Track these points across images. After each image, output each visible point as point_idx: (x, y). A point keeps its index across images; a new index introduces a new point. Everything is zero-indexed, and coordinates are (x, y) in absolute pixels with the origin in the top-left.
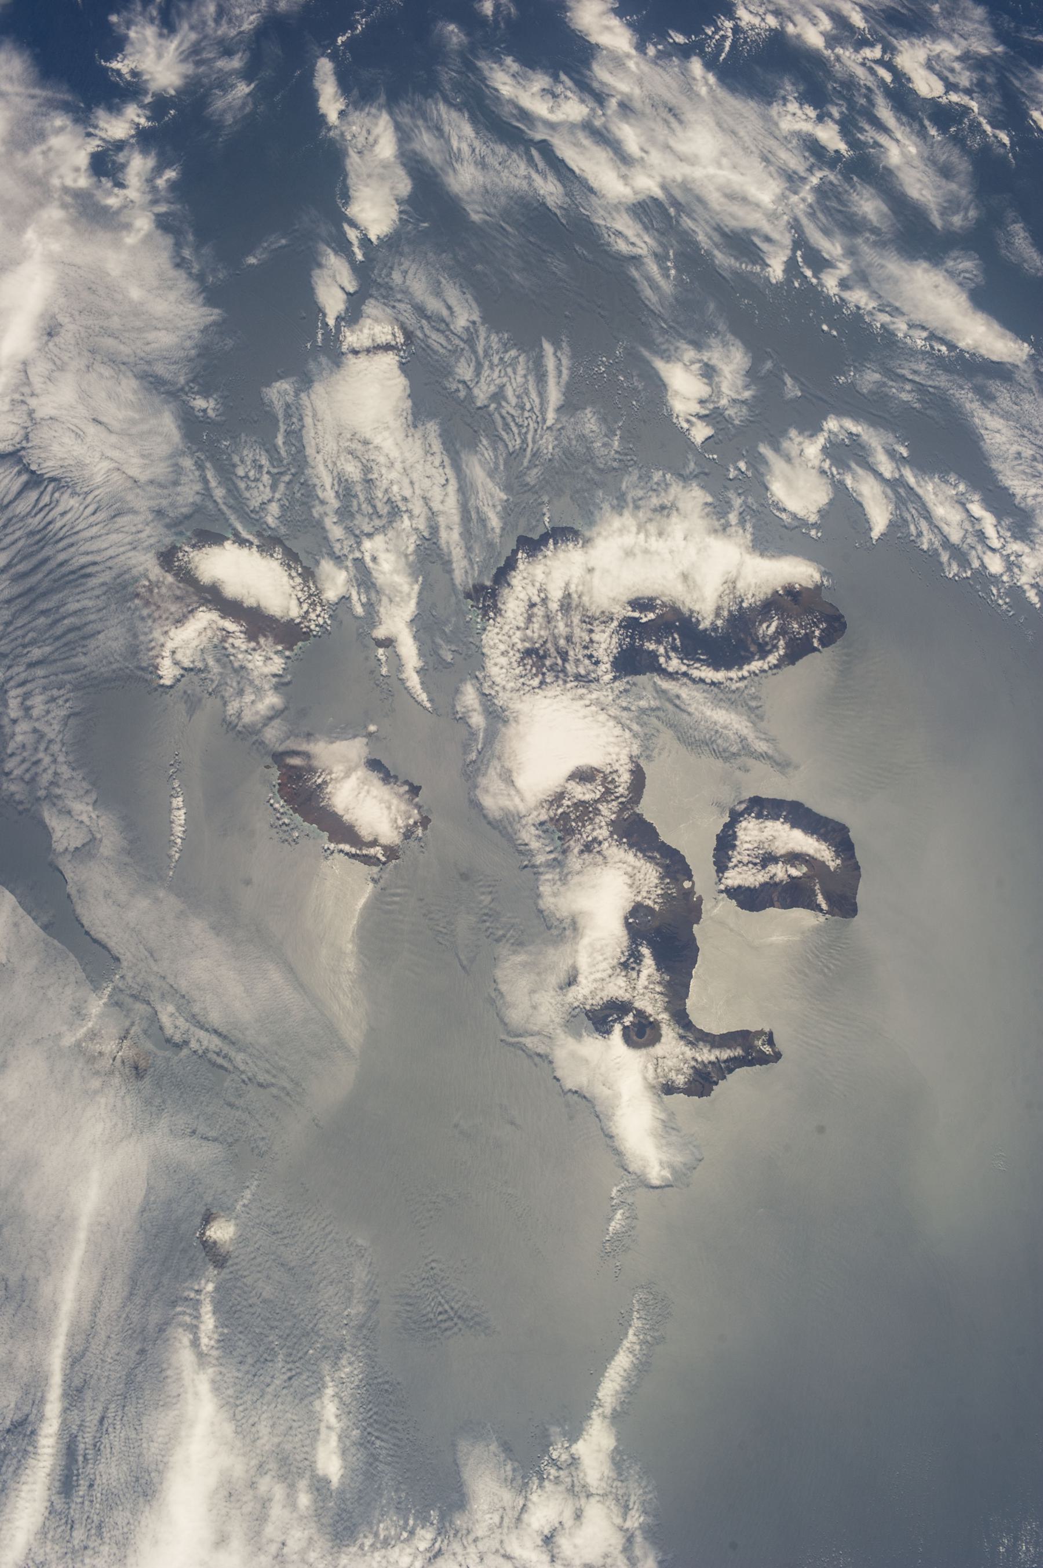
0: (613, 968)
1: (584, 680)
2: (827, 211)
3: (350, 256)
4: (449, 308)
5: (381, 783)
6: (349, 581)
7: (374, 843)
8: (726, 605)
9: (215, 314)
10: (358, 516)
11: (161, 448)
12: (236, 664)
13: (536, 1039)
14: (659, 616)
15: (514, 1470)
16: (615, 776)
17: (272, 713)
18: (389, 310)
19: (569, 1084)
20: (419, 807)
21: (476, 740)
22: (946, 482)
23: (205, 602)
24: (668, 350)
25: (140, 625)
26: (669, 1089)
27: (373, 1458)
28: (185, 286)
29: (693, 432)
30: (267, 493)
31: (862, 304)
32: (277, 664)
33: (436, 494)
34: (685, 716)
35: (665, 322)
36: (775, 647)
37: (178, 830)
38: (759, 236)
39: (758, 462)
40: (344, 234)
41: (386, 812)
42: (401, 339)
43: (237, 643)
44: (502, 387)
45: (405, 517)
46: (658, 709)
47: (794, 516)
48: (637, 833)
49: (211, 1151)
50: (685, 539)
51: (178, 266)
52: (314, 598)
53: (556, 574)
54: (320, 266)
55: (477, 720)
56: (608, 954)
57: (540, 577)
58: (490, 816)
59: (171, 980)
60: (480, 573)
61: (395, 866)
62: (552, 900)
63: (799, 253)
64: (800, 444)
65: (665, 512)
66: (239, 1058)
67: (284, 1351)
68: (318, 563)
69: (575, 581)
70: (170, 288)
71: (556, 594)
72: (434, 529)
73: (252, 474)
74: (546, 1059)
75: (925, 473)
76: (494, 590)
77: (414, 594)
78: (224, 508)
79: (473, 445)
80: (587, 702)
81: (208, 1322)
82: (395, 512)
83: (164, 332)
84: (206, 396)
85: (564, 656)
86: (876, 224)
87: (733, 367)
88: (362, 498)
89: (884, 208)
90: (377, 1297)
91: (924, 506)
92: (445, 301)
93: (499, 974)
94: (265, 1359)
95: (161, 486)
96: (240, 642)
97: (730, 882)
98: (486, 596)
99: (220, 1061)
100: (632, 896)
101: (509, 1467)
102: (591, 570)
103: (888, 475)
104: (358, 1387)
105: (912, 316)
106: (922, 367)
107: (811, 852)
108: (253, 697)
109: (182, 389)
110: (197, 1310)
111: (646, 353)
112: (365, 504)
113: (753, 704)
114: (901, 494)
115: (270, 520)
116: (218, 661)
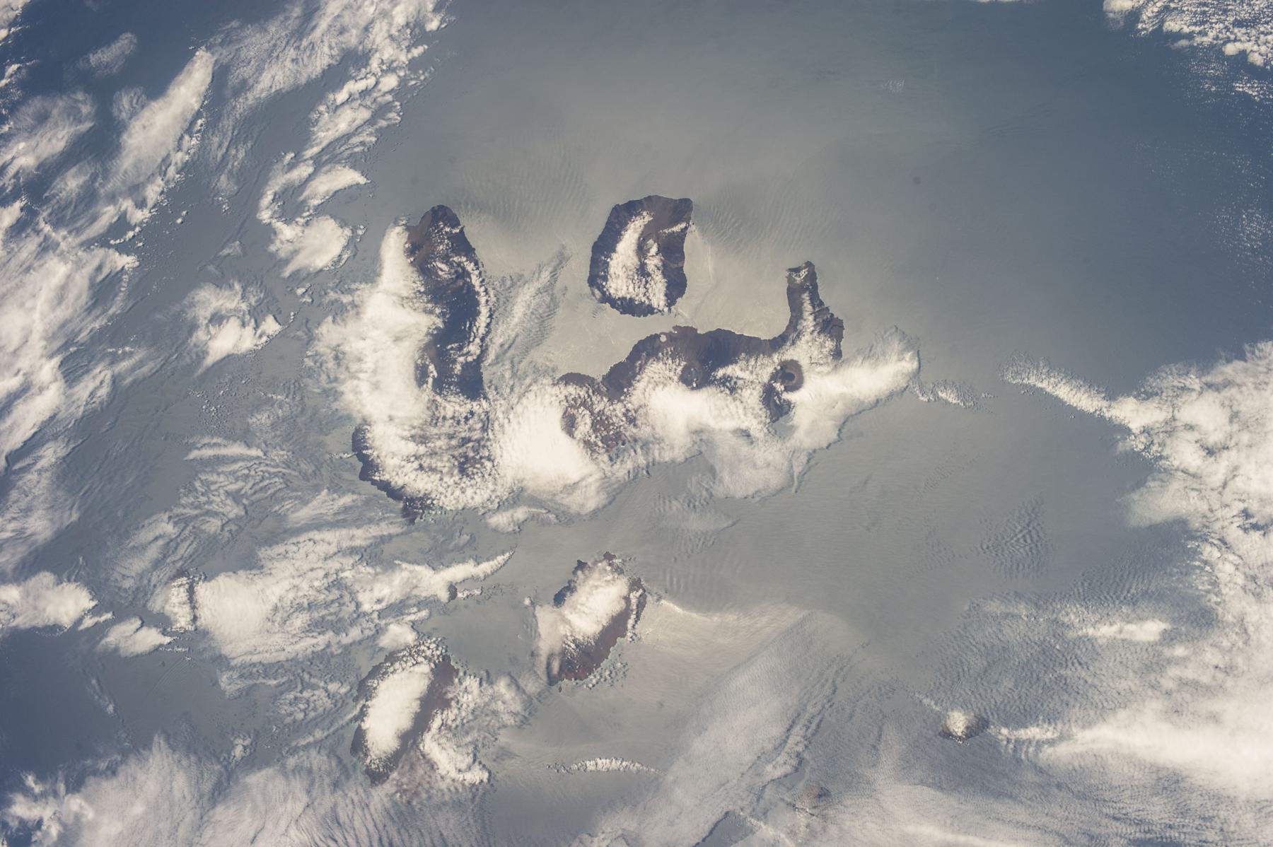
0: (735, 400)
1: (486, 424)
4: (156, 539)
5: (575, 594)
6: (398, 622)
7: (627, 599)
9: (159, 741)
10: (341, 615)
13: (795, 464)
14: (432, 361)
15: (1154, 480)
17: (514, 687)
18: (158, 591)
19: (834, 436)
20: (595, 563)
22: (317, 121)
23: (415, 745)
26: (837, 354)
27: (1146, 594)
29: (270, 332)
30: (320, 693)
31: (159, 190)
32: (471, 683)
33: (322, 549)
34: (518, 340)
35: (171, 355)
36: (459, 264)
37: (615, 764)
38: (96, 276)
39: (297, 277)
40: (87, 629)
41: (600, 590)
42: (184, 580)
43: (452, 717)
44: (228, 494)
47: (346, 248)
48: (620, 380)
49: (891, 734)
52: (413, 652)
53: (394, 448)
54: (116, 650)
55: (521, 513)
57: (396, 461)
58: (604, 502)
60: (391, 512)
62: (676, 451)
63: (112, 242)
66: (811, 710)
68: (381, 649)
69: (400, 432)
71: (411, 448)
72: (353, 551)
73: (302, 707)
74: (812, 455)
75: (309, 139)
77: (411, 567)
78: (332, 730)
79: (281, 518)
81: (1033, 732)
82: (338, 584)
84: (233, 747)
85: (466, 441)
87: (213, 299)
91: (337, 140)
93: (740, 494)
94: (1064, 685)
96: (451, 714)
97: (662, 303)
98: (412, 506)
99: (813, 726)
101: (1152, 484)
102: (391, 419)
103: (311, 170)
104: (1087, 608)
106: (216, 140)
107: (636, 236)
108: (500, 703)
109: (225, 767)
110: (1024, 742)
111: (200, 372)
114: (329, 158)
115: (343, 690)
116: (467, 733)
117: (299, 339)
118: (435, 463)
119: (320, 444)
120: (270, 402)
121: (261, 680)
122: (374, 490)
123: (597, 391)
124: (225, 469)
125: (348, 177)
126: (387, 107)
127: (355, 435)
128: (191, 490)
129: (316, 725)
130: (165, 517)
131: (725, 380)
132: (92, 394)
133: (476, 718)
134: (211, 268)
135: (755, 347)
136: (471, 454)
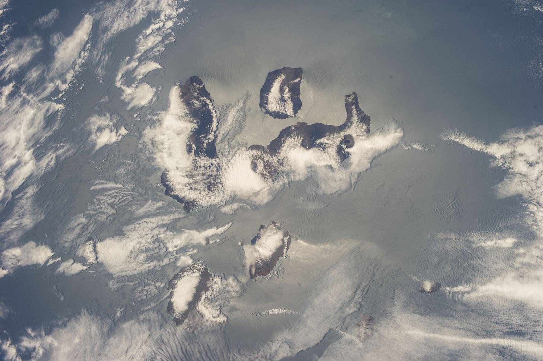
0: (325, 153)
1: (219, 169)
2: (36, 89)
3: (60, 262)
4: (78, 225)
6: (185, 255)
7: (283, 240)
8: (188, 119)
9: (84, 311)
10: (160, 253)
11: (137, 326)
13: (352, 179)
14: (194, 143)
15: (507, 178)
17: (236, 280)
18: (80, 247)
19: (369, 166)
20: (268, 226)
21: (243, 206)
22: (139, 42)
23: (195, 307)
24: (92, 145)
26: (368, 131)
27: (506, 227)
30: (152, 287)
31: (72, 75)
32: (217, 279)
33: (150, 225)
34: (231, 132)
35: (81, 146)
36: (203, 101)
37: (281, 311)
38: (46, 114)
39: (134, 109)
40: (51, 265)
41: (271, 237)
42: (91, 242)
43: (210, 294)
44: (108, 204)
45: (159, 236)
46: (228, 141)
47: (154, 96)
48: (275, 147)
49: (399, 293)
51: (65, 326)
52: (192, 268)
53: (179, 181)
54: (64, 273)
55: (235, 206)
56: (320, 155)
58: (271, 199)
59: (337, 310)
62: (301, 176)
64: (126, 95)
65: (154, 142)
66: (364, 283)
67: (469, 261)
68: (178, 267)
69: (181, 174)
70: (74, 328)
71: (187, 180)
72: (163, 226)
73: (145, 293)
74: (359, 174)
75: (136, 50)
76: (186, 203)
78: (158, 303)
79: (132, 213)
81: (460, 288)
82: (158, 240)
84: (116, 312)
85: (210, 176)
86: (41, 72)
87: (98, 121)
88: (153, 252)
89: (35, 69)
91: (148, 50)
92: (76, 227)
93: (329, 193)
94: (473, 268)
95: (151, 326)
96: (209, 293)
97: (292, 113)
98: (188, 205)
99: (365, 290)
100: (298, 148)
101: (506, 180)
102: (177, 168)
103: (137, 63)
104: (481, 234)
105: (76, 57)
106: (95, 53)
107: (279, 85)
108: (230, 287)
109: (113, 321)
110: (456, 293)
111: (94, 152)
113: (225, 108)
114: (145, 58)
115: (162, 285)
116: (217, 301)
117: (136, 136)
119: (147, 181)
120: (125, 164)
121: (127, 283)
122: (171, 199)
123: (265, 152)
126: (169, 35)
128: (92, 203)
130: (82, 215)
131: (321, 145)
132: (47, 164)
134: (96, 108)
135: (333, 130)
136: (213, 182)
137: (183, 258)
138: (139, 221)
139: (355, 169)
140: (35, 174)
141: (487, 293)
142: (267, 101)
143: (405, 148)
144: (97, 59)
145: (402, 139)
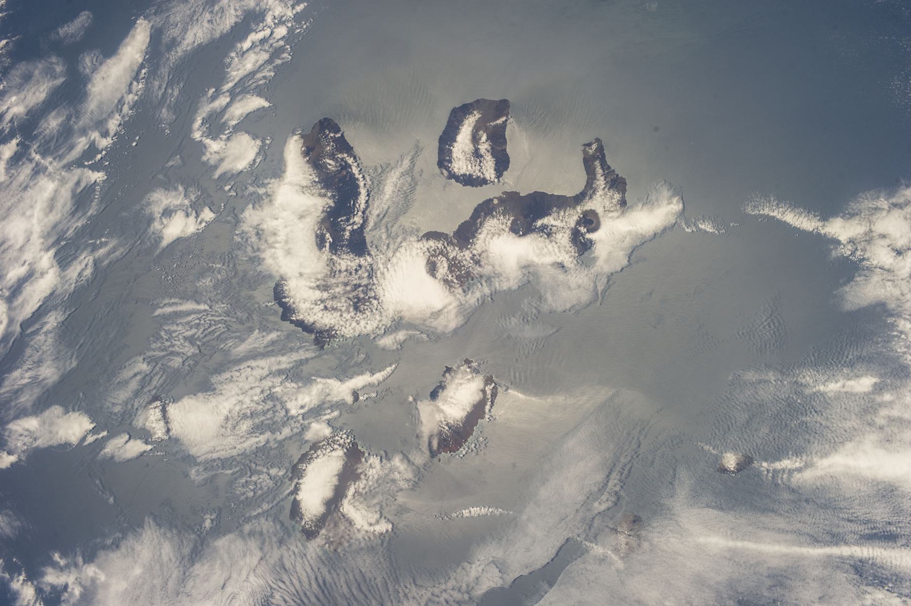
0: (551, 241)
1: (371, 274)
2: (57, 148)
3: (105, 440)
4: (135, 375)
6: (318, 421)
10: (275, 419)
11: (239, 544)
12: (376, 485)
13: (598, 284)
14: (328, 231)
16: (431, 250)
17: (405, 461)
18: (139, 412)
19: (625, 262)
20: (458, 367)
22: (230, 64)
23: (337, 508)
25: (354, 547)
26: (623, 203)
28: (131, 540)
29: (208, 219)
30: (264, 477)
31: (118, 123)
32: (374, 461)
33: (258, 373)
34: (390, 210)
36: (342, 159)
37: (484, 511)
39: (226, 177)
40: (90, 444)
41: (464, 386)
42: (158, 403)
43: (362, 486)
44: (185, 338)
45: (274, 390)
46: (387, 227)
47: (258, 154)
48: (466, 234)
49: (683, 474)
50: (277, 219)
51: (118, 547)
52: (330, 442)
53: (305, 296)
54: (112, 457)
55: (401, 335)
57: (307, 305)
58: (463, 322)
59: (578, 506)
61: (497, 377)
62: (511, 282)
65: (261, 232)
66: (623, 460)
67: (800, 417)
68: (307, 441)
69: (308, 284)
70: (133, 549)
71: (318, 294)
72: (280, 372)
73: (252, 487)
74: (610, 276)
76: (317, 332)
77: (323, 381)
78: (275, 502)
79: (226, 353)
80: (386, 270)
81: (786, 464)
82: (271, 397)
83: (162, 551)
85: (357, 286)
86: (64, 118)
87: (163, 198)
90: (763, 365)
92: (131, 378)
93: (560, 309)
95: (263, 543)
96: (361, 484)
97: (493, 176)
98: (322, 337)
99: (626, 472)
100: (506, 234)
102: (301, 275)
103: (228, 99)
104: (818, 371)
107: (470, 129)
108: (396, 473)
109: (199, 536)
111: (158, 251)
112: (267, 416)
113: (380, 170)
114: (241, 89)
115: (281, 473)
116: (374, 497)
117: (229, 222)
118: (336, 304)
119: (251, 297)
121: (220, 471)
122: (292, 327)
123: (450, 243)
124: (182, 321)
125: (256, 102)
127: (275, 289)
128: (158, 338)
129: (263, 500)
130: (141, 359)
131: (543, 228)
132: (80, 275)
133: (379, 486)
134: (161, 176)
137: (315, 426)
138: (239, 365)
139: (602, 268)
140: (58, 292)
141: (831, 470)
142: (451, 156)
143: (687, 230)
144: (160, 94)
145: (682, 213)
